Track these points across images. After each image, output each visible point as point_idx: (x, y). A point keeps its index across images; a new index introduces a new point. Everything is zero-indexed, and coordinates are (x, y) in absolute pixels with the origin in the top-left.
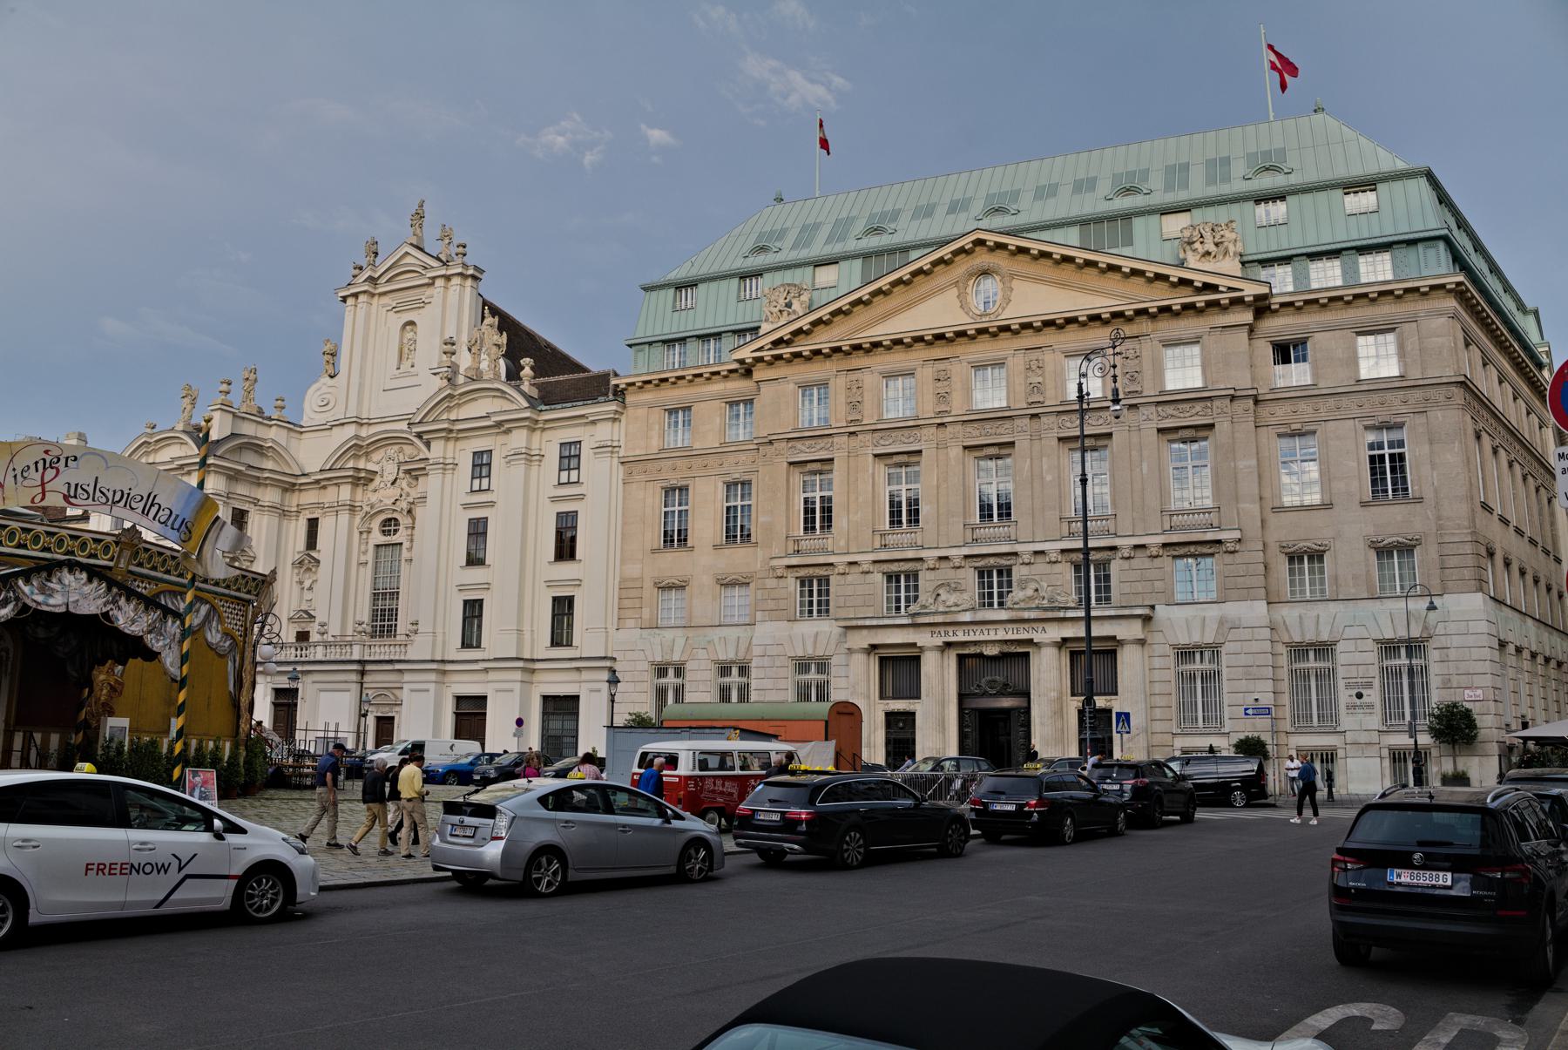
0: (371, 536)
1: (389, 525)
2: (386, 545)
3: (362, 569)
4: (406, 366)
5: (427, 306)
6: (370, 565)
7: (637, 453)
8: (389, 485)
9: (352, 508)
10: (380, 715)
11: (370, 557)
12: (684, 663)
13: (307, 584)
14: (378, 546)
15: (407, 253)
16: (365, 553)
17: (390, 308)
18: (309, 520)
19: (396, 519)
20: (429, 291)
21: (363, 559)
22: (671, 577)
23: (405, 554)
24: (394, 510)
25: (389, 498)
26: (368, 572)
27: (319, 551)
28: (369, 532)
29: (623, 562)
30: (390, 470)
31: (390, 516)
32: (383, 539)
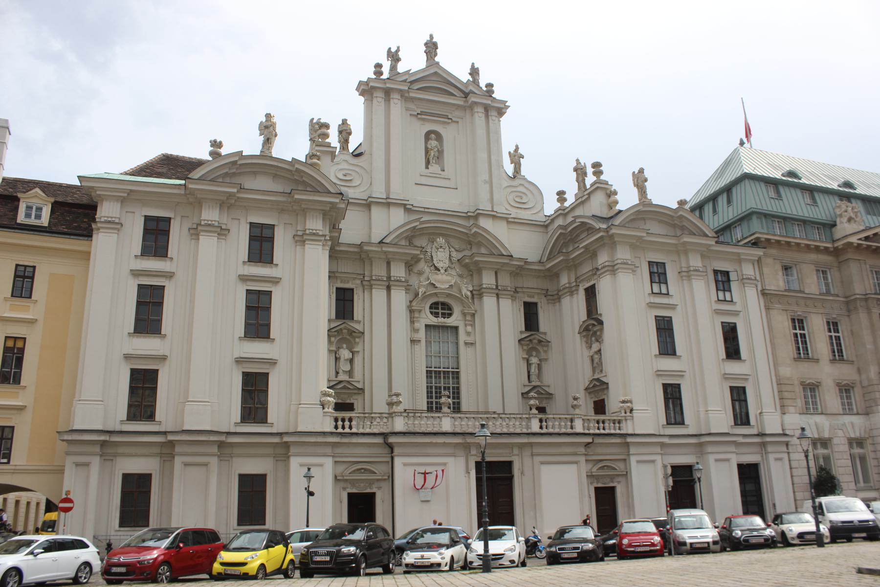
0: (423, 315)
1: (441, 308)
2: (434, 327)
3: (417, 347)
4: (434, 168)
5: (454, 125)
6: (423, 342)
7: (773, 288)
8: (442, 271)
9: (408, 288)
10: (600, 485)
11: (422, 335)
12: (830, 439)
13: (345, 354)
14: (426, 326)
15: (436, 73)
16: (416, 331)
17: (416, 113)
18: (337, 289)
19: (443, 304)
20: (458, 113)
21: (416, 336)
22: (810, 379)
23: (462, 337)
24: (449, 295)
25: (442, 282)
26: (421, 350)
27: (358, 322)
28: (420, 311)
29: (776, 365)
30: (441, 257)
31: (441, 300)
32: (433, 320)
